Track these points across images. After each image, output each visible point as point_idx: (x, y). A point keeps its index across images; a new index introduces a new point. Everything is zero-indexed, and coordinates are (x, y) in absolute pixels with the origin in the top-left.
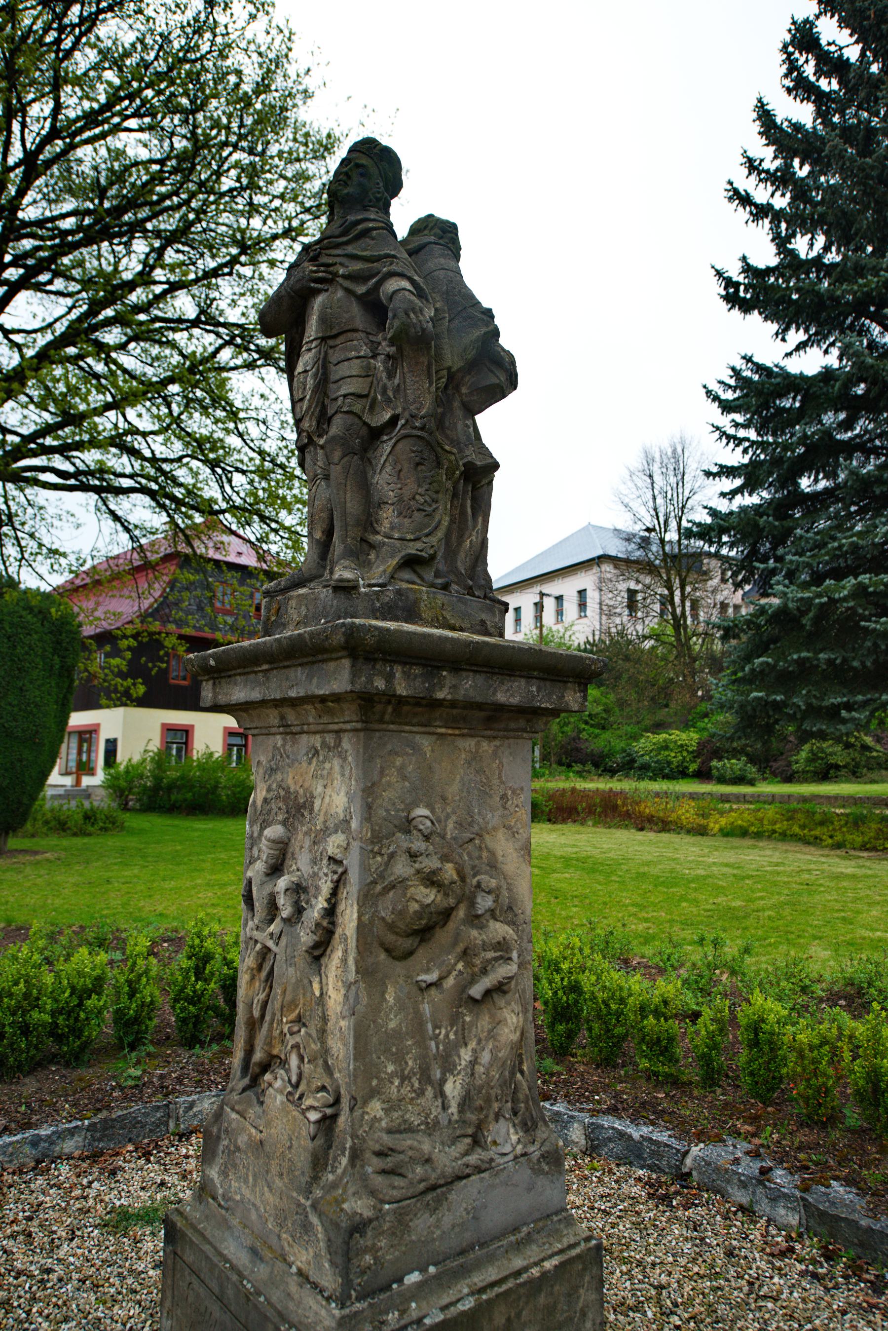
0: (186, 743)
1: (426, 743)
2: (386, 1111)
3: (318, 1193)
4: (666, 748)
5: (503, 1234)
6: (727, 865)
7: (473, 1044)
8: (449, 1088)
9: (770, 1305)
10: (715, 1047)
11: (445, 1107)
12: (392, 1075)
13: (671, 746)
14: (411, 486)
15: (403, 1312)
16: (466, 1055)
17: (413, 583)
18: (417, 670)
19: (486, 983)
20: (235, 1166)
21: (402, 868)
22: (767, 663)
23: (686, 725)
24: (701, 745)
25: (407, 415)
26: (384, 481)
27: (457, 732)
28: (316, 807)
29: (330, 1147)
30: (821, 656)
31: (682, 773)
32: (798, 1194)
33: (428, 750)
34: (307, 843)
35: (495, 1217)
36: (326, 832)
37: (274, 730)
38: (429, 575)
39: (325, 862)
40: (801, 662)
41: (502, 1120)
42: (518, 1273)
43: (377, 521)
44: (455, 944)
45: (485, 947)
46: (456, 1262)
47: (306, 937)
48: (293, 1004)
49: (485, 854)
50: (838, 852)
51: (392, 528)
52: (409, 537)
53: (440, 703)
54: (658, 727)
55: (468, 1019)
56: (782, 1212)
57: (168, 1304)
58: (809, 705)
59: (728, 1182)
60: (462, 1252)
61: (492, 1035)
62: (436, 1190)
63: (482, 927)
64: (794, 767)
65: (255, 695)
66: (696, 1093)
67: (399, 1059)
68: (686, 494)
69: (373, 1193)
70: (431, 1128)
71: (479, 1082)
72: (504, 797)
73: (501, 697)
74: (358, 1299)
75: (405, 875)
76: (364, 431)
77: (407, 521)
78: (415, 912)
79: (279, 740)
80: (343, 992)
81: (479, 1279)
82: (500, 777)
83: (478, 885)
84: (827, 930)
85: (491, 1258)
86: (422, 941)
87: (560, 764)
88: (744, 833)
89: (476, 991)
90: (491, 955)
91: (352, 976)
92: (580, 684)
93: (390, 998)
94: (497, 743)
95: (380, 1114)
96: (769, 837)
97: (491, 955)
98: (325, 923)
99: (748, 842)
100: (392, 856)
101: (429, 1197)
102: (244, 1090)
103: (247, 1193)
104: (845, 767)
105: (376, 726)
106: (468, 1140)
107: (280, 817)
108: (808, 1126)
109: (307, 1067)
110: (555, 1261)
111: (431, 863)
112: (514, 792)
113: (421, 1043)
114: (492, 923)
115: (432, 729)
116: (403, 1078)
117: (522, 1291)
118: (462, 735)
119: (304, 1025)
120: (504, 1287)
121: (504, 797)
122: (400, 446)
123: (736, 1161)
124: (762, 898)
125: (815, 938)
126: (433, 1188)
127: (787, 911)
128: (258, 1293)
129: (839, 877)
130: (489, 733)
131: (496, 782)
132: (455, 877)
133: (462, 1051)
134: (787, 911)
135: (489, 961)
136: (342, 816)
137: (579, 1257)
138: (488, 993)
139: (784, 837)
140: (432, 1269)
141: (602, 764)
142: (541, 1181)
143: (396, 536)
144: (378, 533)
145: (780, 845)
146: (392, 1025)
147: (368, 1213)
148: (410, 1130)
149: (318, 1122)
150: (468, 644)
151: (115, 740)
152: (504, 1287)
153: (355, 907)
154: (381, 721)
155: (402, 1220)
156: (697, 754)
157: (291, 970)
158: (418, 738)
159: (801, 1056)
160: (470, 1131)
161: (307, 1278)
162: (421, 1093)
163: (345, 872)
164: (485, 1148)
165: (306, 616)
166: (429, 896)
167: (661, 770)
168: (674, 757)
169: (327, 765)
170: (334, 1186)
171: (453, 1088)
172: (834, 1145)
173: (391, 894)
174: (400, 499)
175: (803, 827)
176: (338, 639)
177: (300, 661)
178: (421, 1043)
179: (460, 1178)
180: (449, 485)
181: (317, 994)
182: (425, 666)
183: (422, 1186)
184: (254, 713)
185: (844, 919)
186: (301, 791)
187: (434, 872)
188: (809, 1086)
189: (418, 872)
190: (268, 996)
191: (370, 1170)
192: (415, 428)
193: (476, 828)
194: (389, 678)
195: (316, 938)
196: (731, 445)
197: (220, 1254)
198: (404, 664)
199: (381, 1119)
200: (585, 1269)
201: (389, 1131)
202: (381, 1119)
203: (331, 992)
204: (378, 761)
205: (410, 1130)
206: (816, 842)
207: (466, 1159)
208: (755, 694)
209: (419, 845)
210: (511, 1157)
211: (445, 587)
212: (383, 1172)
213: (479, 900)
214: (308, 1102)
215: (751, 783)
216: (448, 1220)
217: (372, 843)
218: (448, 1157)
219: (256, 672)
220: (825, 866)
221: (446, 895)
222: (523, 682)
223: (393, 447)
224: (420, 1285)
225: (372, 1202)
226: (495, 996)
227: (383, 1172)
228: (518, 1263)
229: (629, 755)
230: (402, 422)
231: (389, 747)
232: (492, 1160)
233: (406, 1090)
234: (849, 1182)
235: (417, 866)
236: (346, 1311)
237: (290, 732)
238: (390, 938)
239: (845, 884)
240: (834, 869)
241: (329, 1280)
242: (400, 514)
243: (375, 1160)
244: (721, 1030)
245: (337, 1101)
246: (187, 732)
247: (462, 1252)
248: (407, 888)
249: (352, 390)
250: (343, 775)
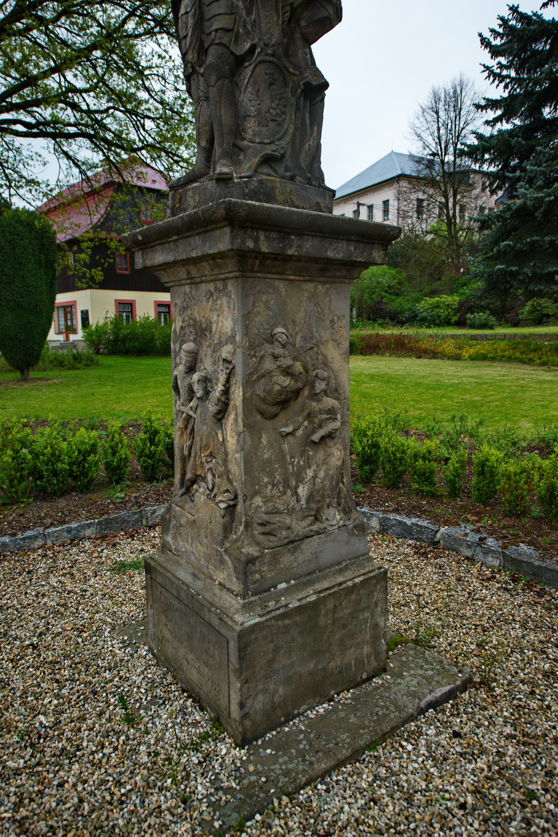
0: (131, 312)
1: (281, 286)
2: (265, 502)
3: (228, 545)
4: (438, 307)
5: (332, 565)
6: (472, 377)
7: (314, 467)
8: (300, 490)
9: (479, 603)
10: (458, 475)
11: (298, 501)
12: (267, 484)
13: (441, 305)
14: (267, 103)
15: (277, 602)
16: (310, 473)
17: (270, 175)
18: (274, 235)
19: (321, 432)
20: (180, 534)
21: (269, 365)
22: (509, 245)
23: (451, 292)
24: (461, 304)
25: (261, 44)
26: (247, 99)
27: (302, 278)
28: (214, 329)
29: (233, 521)
30: (546, 238)
31: (447, 323)
32: (500, 550)
33: (283, 290)
34: (209, 353)
35: (327, 557)
36: (220, 344)
37: (184, 282)
38: (281, 170)
39: (221, 363)
40: (532, 243)
41: (331, 508)
42: (340, 584)
43: (244, 130)
44: (303, 410)
45: (321, 412)
46: (306, 578)
47: (212, 408)
48: (207, 446)
49: (320, 357)
50: (543, 368)
51: (254, 135)
52: (266, 141)
53: (290, 258)
54: (433, 293)
55: (311, 453)
56: (490, 559)
57: (150, 602)
58: (534, 273)
59: (461, 545)
60: (309, 574)
61: (325, 462)
62: (294, 543)
63: (319, 401)
64: (520, 317)
65: (170, 258)
66: (445, 501)
67: (271, 475)
68: (462, 125)
69: (258, 544)
70: (291, 512)
71: (317, 487)
72: (332, 321)
73: (330, 254)
74: (252, 595)
75: (271, 369)
76: (231, 59)
77: (264, 129)
78: (278, 391)
79: (187, 288)
80: (236, 438)
81: (319, 586)
82: (330, 309)
83: (317, 376)
84: (531, 412)
85: (325, 577)
86: (282, 408)
87: (369, 319)
88: (484, 358)
89: (316, 437)
90: (324, 416)
91: (241, 429)
92: (382, 245)
93: (264, 441)
94: (328, 286)
95: (261, 504)
96: (500, 360)
97: (324, 416)
98: (223, 399)
99: (486, 363)
100: (262, 357)
101: (290, 546)
102: (182, 495)
103: (188, 547)
104: (553, 315)
105: (249, 274)
106: (312, 518)
107: (192, 338)
108: (509, 516)
109: (217, 480)
110: (361, 578)
111: (288, 362)
112: (339, 318)
113: (284, 465)
114: (325, 399)
115: (285, 277)
116: (273, 486)
117: (342, 592)
118: (305, 281)
119: (214, 457)
120: (332, 591)
121: (332, 321)
122: (257, 70)
123: (466, 535)
124: (493, 395)
125: (523, 416)
126: (293, 542)
127: (508, 402)
128: (199, 595)
129: (541, 382)
130: (323, 279)
131: (327, 311)
132: (302, 370)
133: (308, 471)
134: (508, 402)
135: (323, 420)
136: (230, 334)
137: (374, 577)
138: (323, 438)
139: (510, 359)
140: (293, 582)
141: (396, 319)
142: (353, 539)
143: (257, 141)
144: (244, 139)
145: (507, 365)
146: (266, 456)
147: (256, 554)
148: (278, 512)
149: (225, 508)
150: (309, 216)
151: (87, 311)
152: (332, 591)
153: (241, 389)
154: (252, 271)
155: (275, 558)
156: (457, 310)
157: (205, 427)
158: (276, 283)
159: (509, 479)
160: (313, 513)
161: (224, 586)
162: (284, 493)
163: (234, 368)
164: (322, 522)
165: (199, 202)
166: (286, 381)
167: (434, 321)
168: (443, 312)
169: (219, 302)
170: (237, 541)
171: (303, 491)
172: (523, 526)
173: (263, 380)
174: (259, 112)
175: (522, 353)
176: (221, 212)
177: (197, 231)
178: (284, 465)
179: (308, 537)
180: (293, 100)
181: (221, 440)
182: (280, 232)
183: (286, 541)
185: (543, 406)
186: (203, 320)
187: (289, 367)
188: (512, 495)
189: (279, 367)
191: (256, 532)
192: (268, 55)
193: (315, 341)
194: (256, 240)
195: (218, 408)
196: (497, 82)
197: (176, 577)
198: (266, 230)
199: (261, 507)
200: (377, 583)
201: (266, 513)
202: (261, 507)
203: (229, 438)
204: (251, 297)
205: (278, 512)
206: (530, 362)
207: (311, 528)
208: (499, 266)
209: (279, 350)
210: (336, 527)
211: (292, 178)
212: (264, 533)
213: (317, 384)
214: (219, 498)
215: (492, 328)
216: (301, 558)
217: (250, 349)
218: (300, 526)
219: (169, 242)
220: (534, 376)
221: (297, 381)
222: (345, 243)
223: (253, 71)
224: (286, 589)
225: (258, 548)
226: (327, 440)
227: (264, 533)
228: (340, 579)
229: (414, 312)
230: (258, 50)
231: (258, 288)
232: (325, 528)
233: (275, 492)
234: (529, 544)
235: (278, 363)
236: (247, 601)
237: (194, 283)
238: (263, 406)
239: (545, 386)
240: (539, 378)
241: (236, 586)
242: (259, 124)
243: (259, 528)
244: (462, 467)
245: (236, 497)
246: (131, 304)
247: (309, 574)
248: (272, 377)
249: (220, 26)
250: (229, 308)
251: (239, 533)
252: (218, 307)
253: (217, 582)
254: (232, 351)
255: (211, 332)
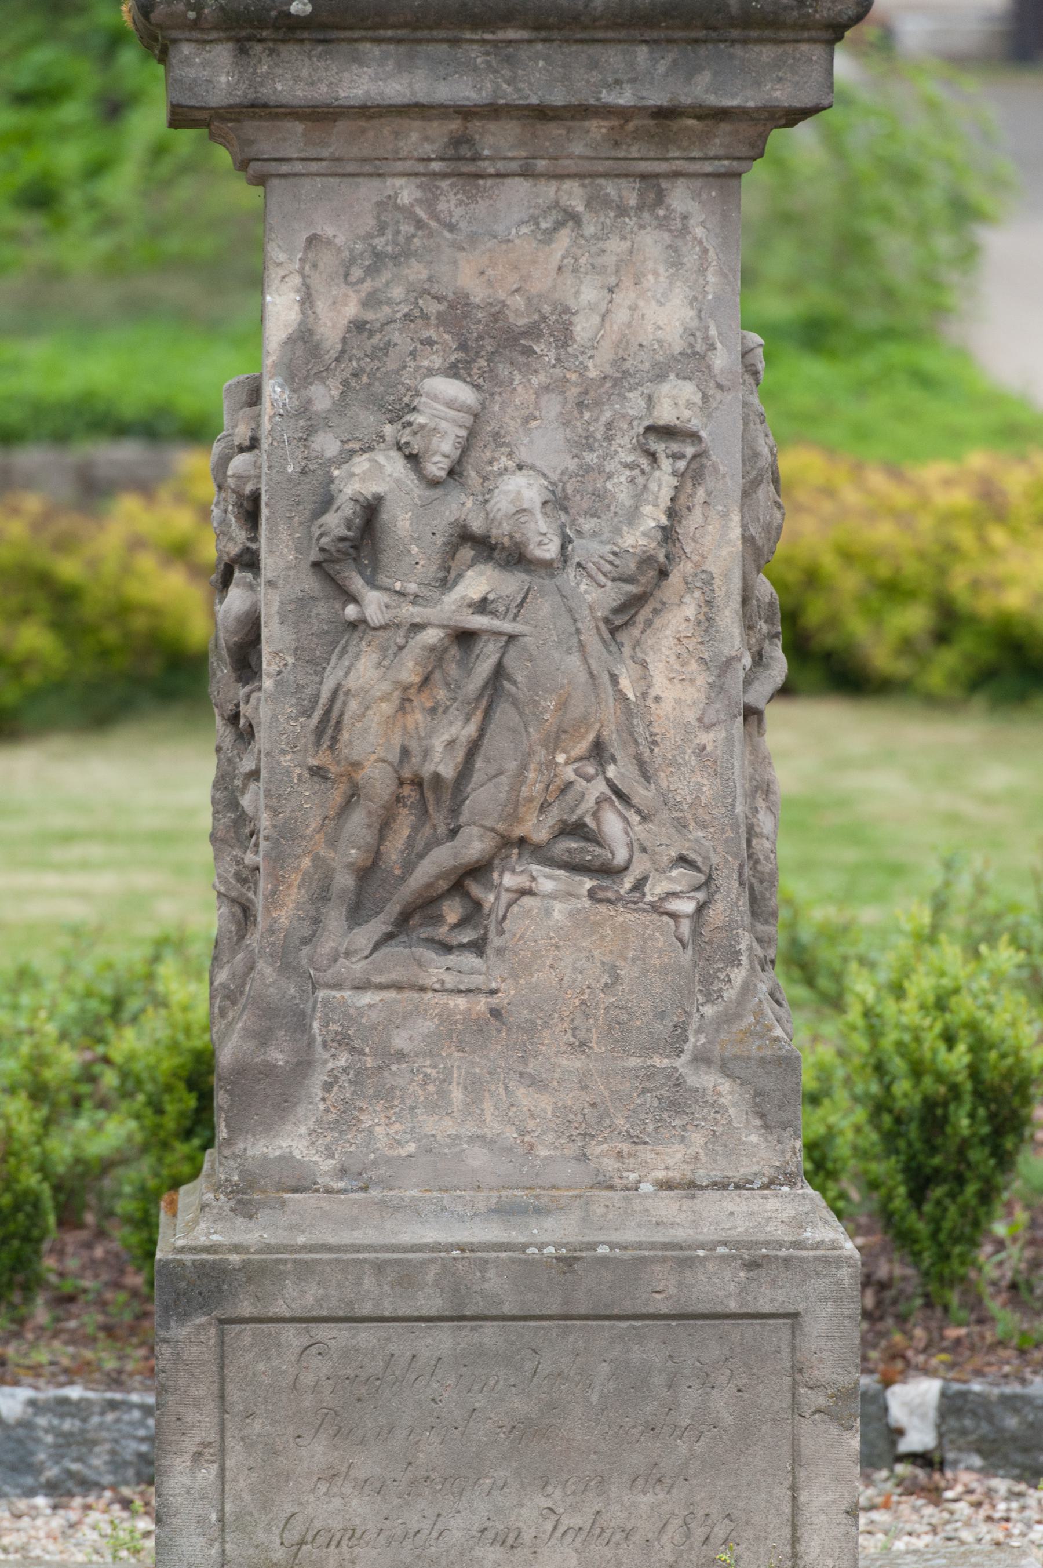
3: (694, 1041)
28: (583, 328)
34: (552, 407)
36: (620, 379)
48: (584, 722)
79: (407, 193)
80: (703, 679)
102: (376, 947)
103: (440, 1127)
109: (640, 830)
161: (692, 1185)
169: (616, 246)
170: (728, 1018)
184: (342, 125)
186: (518, 301)
190: (482, 731)
203: (660, 684)
214: (654, 890)
219: (455, 42)
250: (676, 264)
251: (730, 994)
252: (609, 260)
253: (646, 1187)
254: (697, 399)
255: (564, 337)
